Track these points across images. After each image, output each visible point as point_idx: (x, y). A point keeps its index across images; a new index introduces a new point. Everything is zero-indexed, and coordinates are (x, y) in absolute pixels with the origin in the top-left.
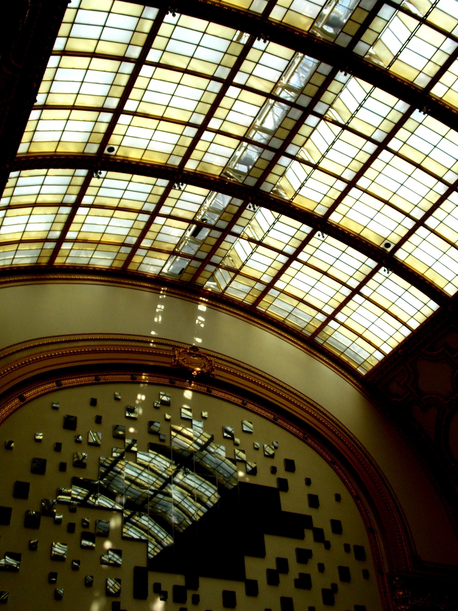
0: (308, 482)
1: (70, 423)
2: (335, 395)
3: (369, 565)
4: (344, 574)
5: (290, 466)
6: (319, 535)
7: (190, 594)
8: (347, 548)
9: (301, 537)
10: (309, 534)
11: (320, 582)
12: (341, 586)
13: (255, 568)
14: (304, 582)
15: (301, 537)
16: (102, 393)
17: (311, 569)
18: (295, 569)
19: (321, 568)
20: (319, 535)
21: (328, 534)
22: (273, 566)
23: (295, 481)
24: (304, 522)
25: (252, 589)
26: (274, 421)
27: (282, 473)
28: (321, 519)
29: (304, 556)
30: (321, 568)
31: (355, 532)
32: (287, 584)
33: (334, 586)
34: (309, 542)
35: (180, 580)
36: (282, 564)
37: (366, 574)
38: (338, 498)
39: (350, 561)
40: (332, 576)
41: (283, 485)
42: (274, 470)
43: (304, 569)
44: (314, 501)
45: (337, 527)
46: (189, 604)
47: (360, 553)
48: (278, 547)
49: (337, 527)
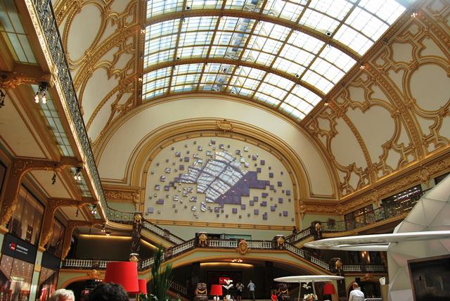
0: (270, 168)
2: (283, 132)
4: (281, 201)
5: (263, 163)
6: (272, 188)
7: (220, 210)
8: (283, 192)
9: (265, 189)
10: (268, 188)
11: (270, 204)
12: (278, 204)
13: (245, 201)
14: (264, 204)
15: (265, 189)
16: (190, 142)
17: (267, 200)
18: (261, 200)
20: (272, 188)
22: (252, 199)
23: (265, 170)
24: (267, 183)
25: (244, 208)
26: (258, 146)
27: (259, 166)
28: (273, 182)
29: (265, 195)
30: (271, 199)
31: (288, 185)
32: (257, 206)
33: (276, 206)
34: (267, 190)
35: (217, 205)
36: (256, 199)
37: (290, 200)
38: (282, 173)
40: (276, 201)
41: (259, 170)
42: (256, 165)
43: (264, 200)
44: (271, 176)
45: (280, 184)
46: (220, 213)
47: (288, 194)
48: (254, 193)
49: (280, 184)
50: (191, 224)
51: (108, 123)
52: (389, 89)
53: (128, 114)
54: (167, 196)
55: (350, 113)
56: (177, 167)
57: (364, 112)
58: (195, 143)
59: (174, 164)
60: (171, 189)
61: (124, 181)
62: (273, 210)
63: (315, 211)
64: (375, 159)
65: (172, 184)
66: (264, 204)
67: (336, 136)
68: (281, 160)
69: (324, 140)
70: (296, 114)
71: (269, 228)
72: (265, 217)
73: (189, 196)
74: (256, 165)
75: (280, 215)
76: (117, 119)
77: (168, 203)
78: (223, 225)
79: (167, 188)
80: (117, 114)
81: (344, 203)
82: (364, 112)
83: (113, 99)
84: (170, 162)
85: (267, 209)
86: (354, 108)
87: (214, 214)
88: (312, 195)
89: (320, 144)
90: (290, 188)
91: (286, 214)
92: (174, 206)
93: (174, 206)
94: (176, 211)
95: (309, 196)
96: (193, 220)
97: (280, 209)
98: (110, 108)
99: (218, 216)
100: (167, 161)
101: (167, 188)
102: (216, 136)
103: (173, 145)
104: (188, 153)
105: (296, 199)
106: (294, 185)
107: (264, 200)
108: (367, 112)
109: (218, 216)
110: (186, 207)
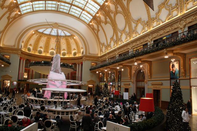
52: (110, 18)
55: (102, 24)
57: (105, 25)
61: (14, 46)
63: (89, 60)
64: (109, 44)
67: (100, 31)
69: (96, 32)
70: (86, 21)
76: (12, 21)
80: (11, 20)
81: (101, 57)
82: (105, 25)
83: (7, 15)
86: (103, 23)
88: (89, 53)
89: (95, 33)
108: (106, 25)
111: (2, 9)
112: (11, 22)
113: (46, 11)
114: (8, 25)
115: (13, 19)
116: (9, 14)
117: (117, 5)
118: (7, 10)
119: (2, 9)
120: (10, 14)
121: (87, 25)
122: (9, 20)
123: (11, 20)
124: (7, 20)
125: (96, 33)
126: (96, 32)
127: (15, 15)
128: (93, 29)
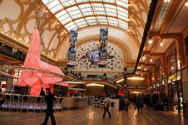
0: (115, 51)
1: (82, 49)
3: (123, 61)
4: (118, 63)
9: (112, 58)
10: (114, 58)
14: (112, 64)
15: (112, 58)
16: (86, 45)
17: (113, 63)
19: (115, 62)
21: (117, 58)
23: (113, 52)
24: (113, 56)
28: (116, 56)
29: (112, 61)
30: (115, 62)
33: (116, 65)
34: (114, 59)
37: (122, 62)
38: (120, 52)
39: (120, 61)
40: (117, 63)
42: (110, 50)
43: (112, 63)
45: (119, 56)
46: (96, 68)
47: (122, 60)
50: (86, 72)
51: (59, 42)
53: (66, 38)
54: (79, 63)
56: (82, 53)
58: (88, 45)
59: (81, 52)
60: (80, 61)
62: (115, 66)
63: (132, 66)
65: (80, 59)
66: (112, 64)
68: (120, 47)
71: (113, 72)
72: (112, 69)
73: (86, 63)
74: (110, 50)
75: (118, 68)
76: (63, 40)
77: (79, 65)
78: (97, 72)
79: (78, 61)
80: (61, 39)
84: (80, 52)
85: (113, 66)
87: (94, 68)
88: (131, 60)
89: (136, 39)
90: (123, 58)
91: (120, 68)
92: (81, 66)
93: (81, 66)
94: (81, 68)
95: (130, 59)
96: (87, 70)
97: (118, 65)
98: (57, 38)
99: (95, 69)
100: (79, 52)
101: (78, 61)
102: (96, 41)
103: (81, 46)
104: (86, 48)
105: (125, 62)
106: (125, 56)
107: (112, 63)
109: (95, 69)
110: (84, 66)
111: (51, 31)
112: (62, 42)
113: (89, 26)
114: (60, 44)
115: (63, 38)
116: (58, 34)
117: (137, 3)
118: (55, 31)
119: (51, 31)
120: (59, 34)
121: (128, 33)
122: (60, 40)
123: (61, 39)
124: (58, 40)
125: (136, 38)
126: (136, 37)
127: (64, 34)
128: (133, 35)
